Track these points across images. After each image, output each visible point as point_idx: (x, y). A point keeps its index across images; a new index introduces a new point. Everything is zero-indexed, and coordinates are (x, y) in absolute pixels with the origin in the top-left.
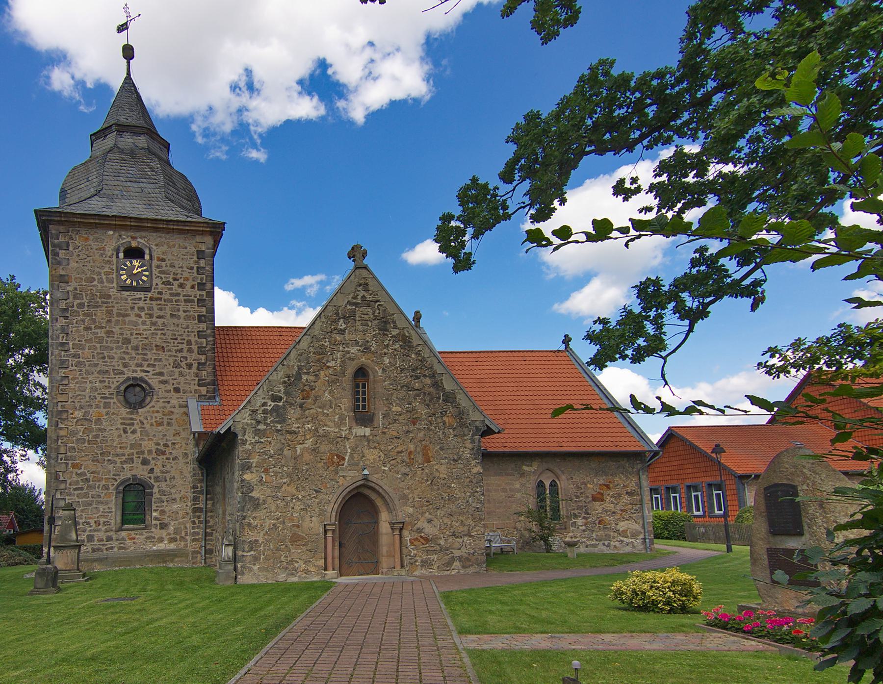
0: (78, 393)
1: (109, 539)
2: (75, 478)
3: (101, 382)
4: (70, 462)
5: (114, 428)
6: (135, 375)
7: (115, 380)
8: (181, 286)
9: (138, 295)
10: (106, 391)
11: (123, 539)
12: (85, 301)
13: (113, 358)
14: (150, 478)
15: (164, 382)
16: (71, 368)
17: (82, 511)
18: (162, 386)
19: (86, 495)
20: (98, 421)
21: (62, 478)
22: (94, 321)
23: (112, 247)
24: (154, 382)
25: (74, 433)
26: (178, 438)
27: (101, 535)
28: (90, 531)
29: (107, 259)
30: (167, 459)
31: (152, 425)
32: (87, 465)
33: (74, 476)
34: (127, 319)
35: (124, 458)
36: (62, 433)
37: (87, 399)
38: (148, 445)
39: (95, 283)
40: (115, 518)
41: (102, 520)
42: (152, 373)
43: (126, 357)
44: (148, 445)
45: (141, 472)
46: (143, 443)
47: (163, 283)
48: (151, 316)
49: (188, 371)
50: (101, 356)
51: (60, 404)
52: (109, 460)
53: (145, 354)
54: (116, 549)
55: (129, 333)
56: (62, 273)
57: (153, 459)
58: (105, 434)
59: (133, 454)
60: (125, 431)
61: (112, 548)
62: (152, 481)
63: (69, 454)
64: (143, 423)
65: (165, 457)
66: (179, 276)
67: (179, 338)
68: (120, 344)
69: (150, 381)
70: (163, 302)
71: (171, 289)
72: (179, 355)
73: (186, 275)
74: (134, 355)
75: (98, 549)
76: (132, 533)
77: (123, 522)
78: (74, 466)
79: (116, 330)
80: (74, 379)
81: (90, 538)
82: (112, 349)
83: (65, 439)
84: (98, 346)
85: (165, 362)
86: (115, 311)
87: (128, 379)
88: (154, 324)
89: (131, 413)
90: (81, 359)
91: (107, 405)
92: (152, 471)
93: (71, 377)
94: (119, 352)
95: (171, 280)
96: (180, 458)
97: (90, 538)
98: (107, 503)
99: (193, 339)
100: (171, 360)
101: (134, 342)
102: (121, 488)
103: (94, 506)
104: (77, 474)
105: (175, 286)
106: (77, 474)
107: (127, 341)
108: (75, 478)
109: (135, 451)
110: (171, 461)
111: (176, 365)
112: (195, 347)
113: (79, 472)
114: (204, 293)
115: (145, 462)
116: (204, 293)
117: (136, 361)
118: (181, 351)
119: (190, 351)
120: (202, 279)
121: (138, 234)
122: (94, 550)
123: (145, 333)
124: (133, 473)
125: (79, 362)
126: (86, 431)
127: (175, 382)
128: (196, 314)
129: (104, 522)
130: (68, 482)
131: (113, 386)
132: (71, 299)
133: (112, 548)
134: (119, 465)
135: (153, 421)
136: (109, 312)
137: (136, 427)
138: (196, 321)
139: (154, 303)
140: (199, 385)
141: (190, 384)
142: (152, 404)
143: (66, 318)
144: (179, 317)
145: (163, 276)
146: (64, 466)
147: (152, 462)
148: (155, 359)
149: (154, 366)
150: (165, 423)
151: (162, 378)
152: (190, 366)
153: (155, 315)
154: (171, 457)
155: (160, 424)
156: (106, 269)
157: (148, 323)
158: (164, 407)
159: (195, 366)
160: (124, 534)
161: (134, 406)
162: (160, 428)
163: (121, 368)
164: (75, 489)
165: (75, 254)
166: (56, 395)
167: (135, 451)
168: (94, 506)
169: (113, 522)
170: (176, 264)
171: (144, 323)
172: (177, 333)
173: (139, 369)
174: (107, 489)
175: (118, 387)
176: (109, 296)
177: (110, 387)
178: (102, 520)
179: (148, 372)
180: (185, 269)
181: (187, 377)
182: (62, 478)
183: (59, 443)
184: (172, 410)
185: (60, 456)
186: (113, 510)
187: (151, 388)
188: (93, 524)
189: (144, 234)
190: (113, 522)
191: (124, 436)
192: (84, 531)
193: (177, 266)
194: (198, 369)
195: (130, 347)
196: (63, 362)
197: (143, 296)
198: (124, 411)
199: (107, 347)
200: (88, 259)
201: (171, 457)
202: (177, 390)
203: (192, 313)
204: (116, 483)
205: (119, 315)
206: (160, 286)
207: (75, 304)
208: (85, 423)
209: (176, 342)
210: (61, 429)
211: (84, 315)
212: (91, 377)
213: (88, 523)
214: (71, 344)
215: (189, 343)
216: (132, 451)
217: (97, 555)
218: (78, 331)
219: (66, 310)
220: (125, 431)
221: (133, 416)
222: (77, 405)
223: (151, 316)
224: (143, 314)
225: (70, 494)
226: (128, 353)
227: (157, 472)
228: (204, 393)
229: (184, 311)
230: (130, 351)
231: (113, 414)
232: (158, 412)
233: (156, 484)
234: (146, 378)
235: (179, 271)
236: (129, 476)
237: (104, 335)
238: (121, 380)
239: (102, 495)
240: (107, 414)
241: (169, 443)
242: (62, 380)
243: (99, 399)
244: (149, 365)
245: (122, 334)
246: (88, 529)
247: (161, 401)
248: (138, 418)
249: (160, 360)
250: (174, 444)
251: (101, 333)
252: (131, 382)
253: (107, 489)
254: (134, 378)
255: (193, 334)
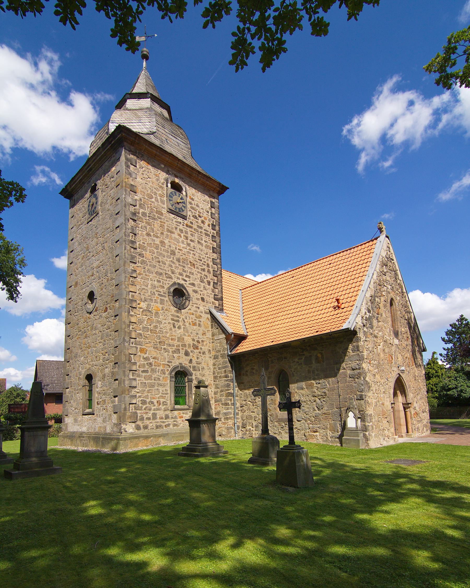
0: (143, 287)
1: (167, 417)
2: (143, 362)
3: (159, 281)
4: (139, 347)
5: (167, 322)
6: (179, 281)
7: (167, 282)
8: (203, 222)
9: (180, 220)
10: (161, 290)
11: (176, 417)
12: (147, 211)
13: (165, 264)
14: (190, 367)
15: (195, 292)
16: (138, 264)
17: (148, 392)
18: (195, 294)
19: (150, 378)
20: (157, 313)
21: (133, 361)
22: (153, 229)
23: (164, 177)
24: (190, 289)
25: (141, 322)
26: (205, 337)
27: (160, 413)
28: (154, 410)
29: (160, 184)
30: (200, 353)
31: (190, 324)
32: (151, 352)
33: (142, 359)
34: (173, 235)
35: (174, 348)
36: (133, 320)
37: (149, 294)
38: (188, 340)
39: (153, 200)
40: (170, 397)
41: (162, 400)
42: (188, 282)
43: (173, 265)
44: (188, 340)
45: (184, 361)
46: (186, 338)
47: (193, 216)
48: (187, 238)
49: (208, 286)
50: (157, 260)
51: (131, 293)
52: (164, 349)
53: (184, 267)
54: (171, 426)
55: (174, 246)
56: (133, 183)
57: (191, 351)
58: (161, 326)
59: (179, 345)
60: (174, 327)
61: (169, 425)
62: (191, 370)
63: (138, 339)
64: (184, 321)
65: (198, 351)
66: (201, 215)
67: (203, 260)
68: (169, 254)
69: (187, 289)
70: (193, 230)
71: (197, 222)
72: (203, 273)
73: (205, 215)
74: (178, 265)
75: (160, 426)
76: (181, 412)
77: (177, 403)
78: (142, 350)
79: (166, 241)
80: (140, 274)
81: (154, 415)
82: (164, 257)
83: (135, 325)
84: (156, 251)
85: (195, 276)
86: (166, 227)
87: (175, 284)
88: (189, 245)
89: (178, 312)
90: (144, 259)
91: (162, 302)
92: (191, 361)
93: (138, 272)
94: (169, 260)
95: (197, 216)
96: (207, 353)
97: (154, 415)
98: (164, 386)
99: (211, 264)
100: (199, 275)
101: (178, 255)
102: (173, 373)
103: (156, 388)
104: (144, 358)
105: (200, 221)
106: (144, 358)
107: (173, 253)
108: (143, 362)
109: (180, 344)
110: (202, 354)
111: (202, 281)
112: (211, 270)
113: (145, 356)
114: (215, 232)
115: (187, 354)
116: (215, 232)
117: (179, 271)
118: (204, 270)
119: (209, 271)
120: (213, 222)
121: (178, 175)
122: (157, 427)
123: (184, 250)
124: (180, 361)
125: (143, 261)
126: (149, 322)
127: (201, 293)
128: (211, 246)
129: (163, 402)
130: (138, 364)
131: (166, 287)
132: (137, 207)
133: (169, 425)
134: (171, 354)
135: (190, 321)
136: (162, 226)
137: (181, 323)
138: (211, 251)
139: (189, 229)
140: (215, 299)
141: (209, 297)
142: (189, 307)
143: (135, 221)
144: (202, 245)
145: (193, 211)
146: (135, 349)
147: (191, 354)
148: (190, 272)
149: (189, 277)
150: (197, 324)
151: (194, 288)
152: (209, 283)
153: (189, 238)
154: (202, 351)
155: (194, 324)
156: (160, 192)
157: (185, 243)
158: (196, 311)
159: (212, 284)
160: (176, 413)
161: (180, 307)
162: (195, 327)
163: (170, 273)
164: (143, 371)
165: (141, 172)
166: (128, 285)
167: (180, 344)
168: (156, 388)
169: (169, 402)
170: (200, 205)
171: (183, 242)
172: (201, 257)
173: (181, 277)
174: (164, 374)
175: (169, 288)
176: (162, 214)
177: (163, 287)
178: (162, 400)
179: (186, 281)
180: (204, 211)
181: (208, 291)
182: (133, 361)
183: (131, 329)
184: (200, 314)
185: (132, 340)
186: (169, 392)
187: (189, 295)
188: (156, 403)
189: (182, 176)
190: (169, 402)
191: (173, 329)
192: (150, 410)
193: (200, 207)
194: (214, 286)
195: (175, 258)
196: (133, 257)
197: (182, 222)
198: (173, 309)
199: (161, 254)
200: (149, 179)
201: (202, 351)
202: (203, 299)
203: (209, 244)
204: (170, 369)
205: (168, 231)
206: (192, 218)
207: (141, 212)
208: (149, 314)
209: (201, 263)
210: (132, 316)
211: (146, 223)
212: (151, 276)
213: (152, 403)
214: (138, 243)
215: (208, 266)
216: (178, 343)
217: (159, 431)
218: (142, 235)
219: (134, 214)
220: (174, 327)
221: (179, 315)
222: (143, 297)
223: (187, 238)
224: (182, 235)
225: (139, 376)
226: (173, 263)
227: (194, 361)
228: (217, 305)
229: (205, 241)
230: (175, 261)
231: (166, 310)
232: (193, 314)
233: (194, 372)
234: (185, 285)
235: (201, 211)
236: (177, 364)
237: (159, 243)
238: (171, 283)
239: (161, 378)
240: (163, 309)
241: (200, 340)
242: (132, 273)
243: (157, 295)
244: (186, 276)
245: (170, 246)
246: (153, 408)
247: (195, 305)
248: (182, 317)
249: (193, 274)
250: (203, 341)
251: (157, 241)
252: (177, 287)
253: (164, 374)
254: (179, 284)
255: (210, 260)
